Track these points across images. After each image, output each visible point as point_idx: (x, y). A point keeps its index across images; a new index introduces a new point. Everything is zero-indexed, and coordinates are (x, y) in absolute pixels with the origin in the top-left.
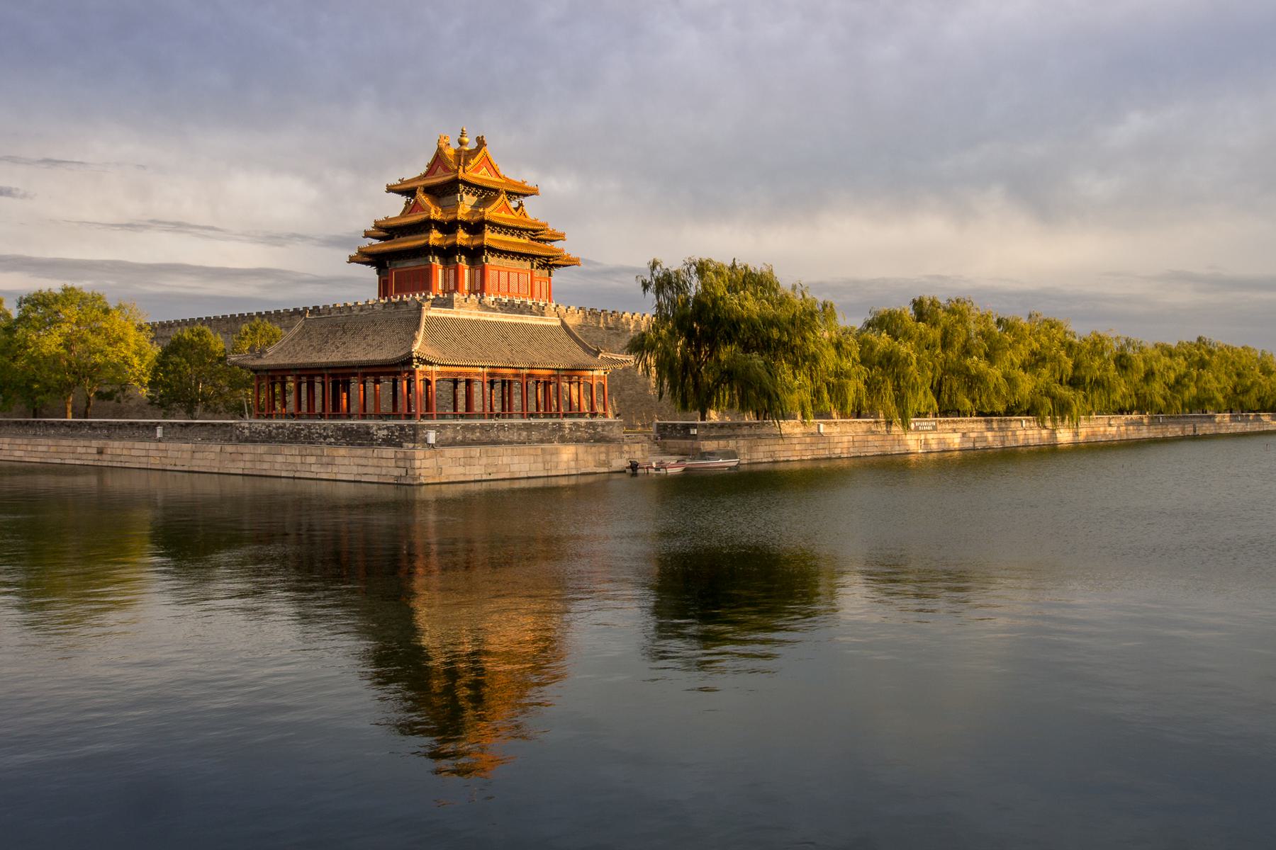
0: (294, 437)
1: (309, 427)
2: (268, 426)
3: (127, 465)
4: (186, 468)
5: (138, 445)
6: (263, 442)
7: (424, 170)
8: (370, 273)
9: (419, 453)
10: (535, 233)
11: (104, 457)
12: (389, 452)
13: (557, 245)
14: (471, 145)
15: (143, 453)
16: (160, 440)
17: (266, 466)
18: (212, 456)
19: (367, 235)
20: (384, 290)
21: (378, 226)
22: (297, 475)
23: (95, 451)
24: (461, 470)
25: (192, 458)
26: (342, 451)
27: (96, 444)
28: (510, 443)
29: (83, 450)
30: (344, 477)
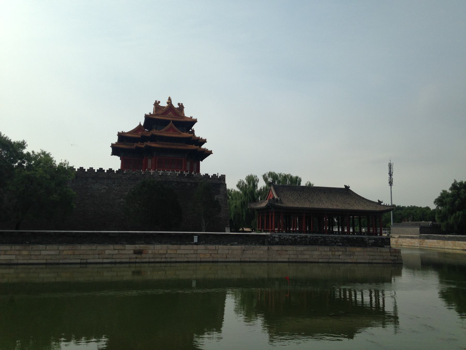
1: (324, 238)
2: (295, 236)
3: (173, 260)
4: (239, 260)
5: (183, 247)
6: (291, 244)
11: (143, 256)
15: (192, 252)
16: (196, 244)
18: (262, 252)
22: (330, 260)
23: (132, 252)
26: (359, 249)
29: (116, 252)
30: (362, 261)
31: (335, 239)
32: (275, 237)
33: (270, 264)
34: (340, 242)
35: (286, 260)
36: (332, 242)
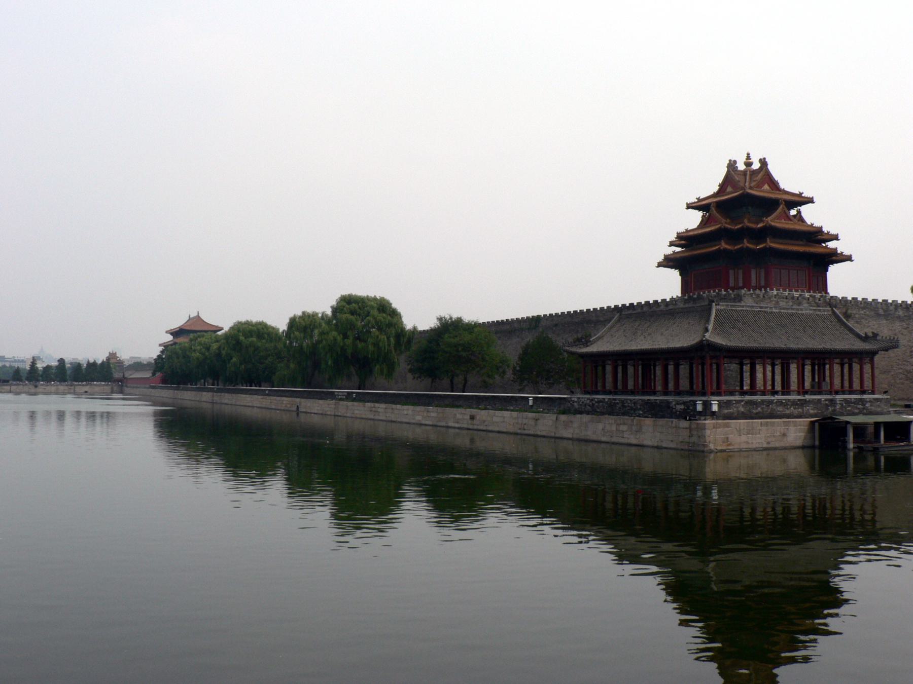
0: (611, 410)
1: (622, 401)
2: (592, 400)
5: (498, 413)
7: (716, 189)
9: (709, 422)
11: (475, 422)
12: (684, 424)
13: (831, 245)
14: (756, 166)
17: (589, 433)
19: (672, 244)
20: (686, 286)
21: (680, 237)
24: (744, 438)
25: (536, 424)
26: (648, 422)
27: (470, 411)
28: (788, 416)
31: (635, 403)
32: (574, 402)
33: (557, 440)
34: (640, 409)
35: (570, 436)
36: (631, 408)
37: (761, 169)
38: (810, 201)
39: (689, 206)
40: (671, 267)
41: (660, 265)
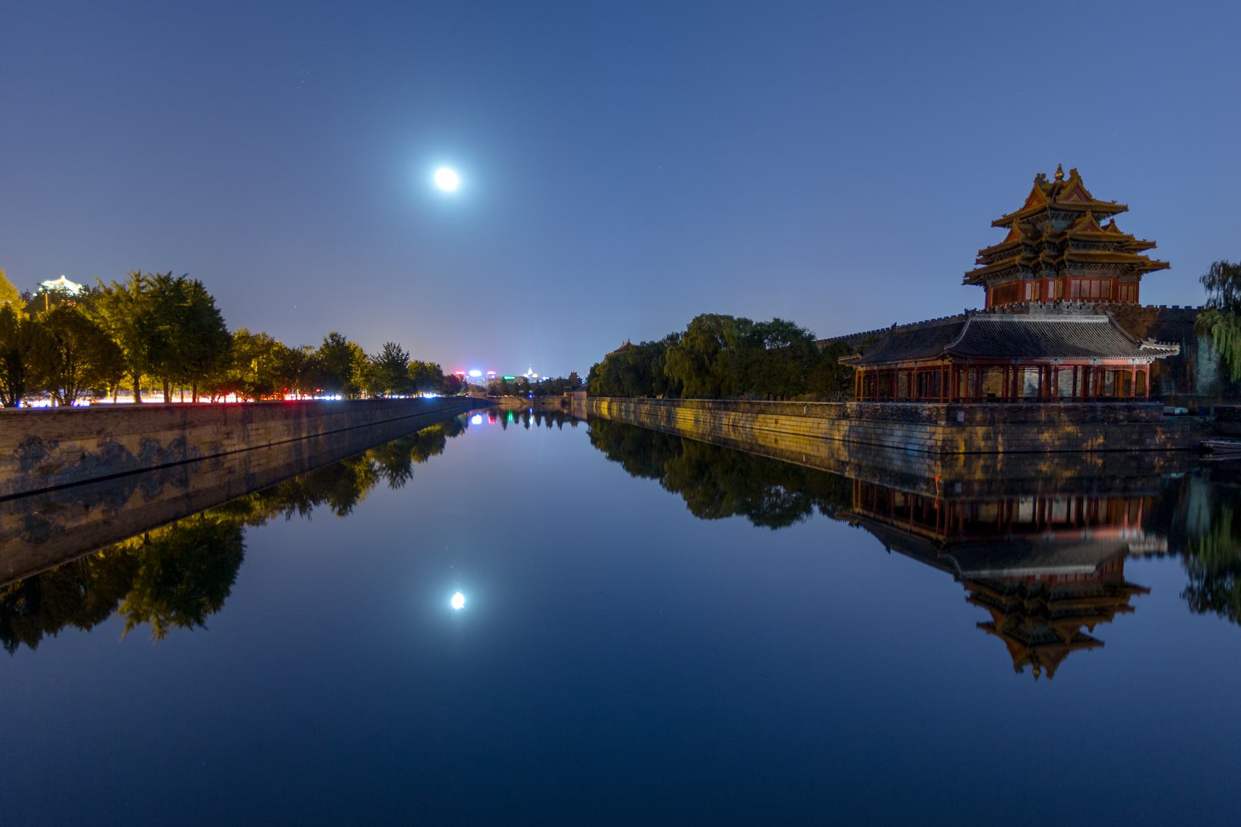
7: (1023, 204)
8: (980, 290)
10: (1126, 244)
19: (978, 262)
21: (981, 253)
37: (1071, 179)
38: (1125, 209)
39: (995, 224)
40: (976, 284)
41: (965, 282)
